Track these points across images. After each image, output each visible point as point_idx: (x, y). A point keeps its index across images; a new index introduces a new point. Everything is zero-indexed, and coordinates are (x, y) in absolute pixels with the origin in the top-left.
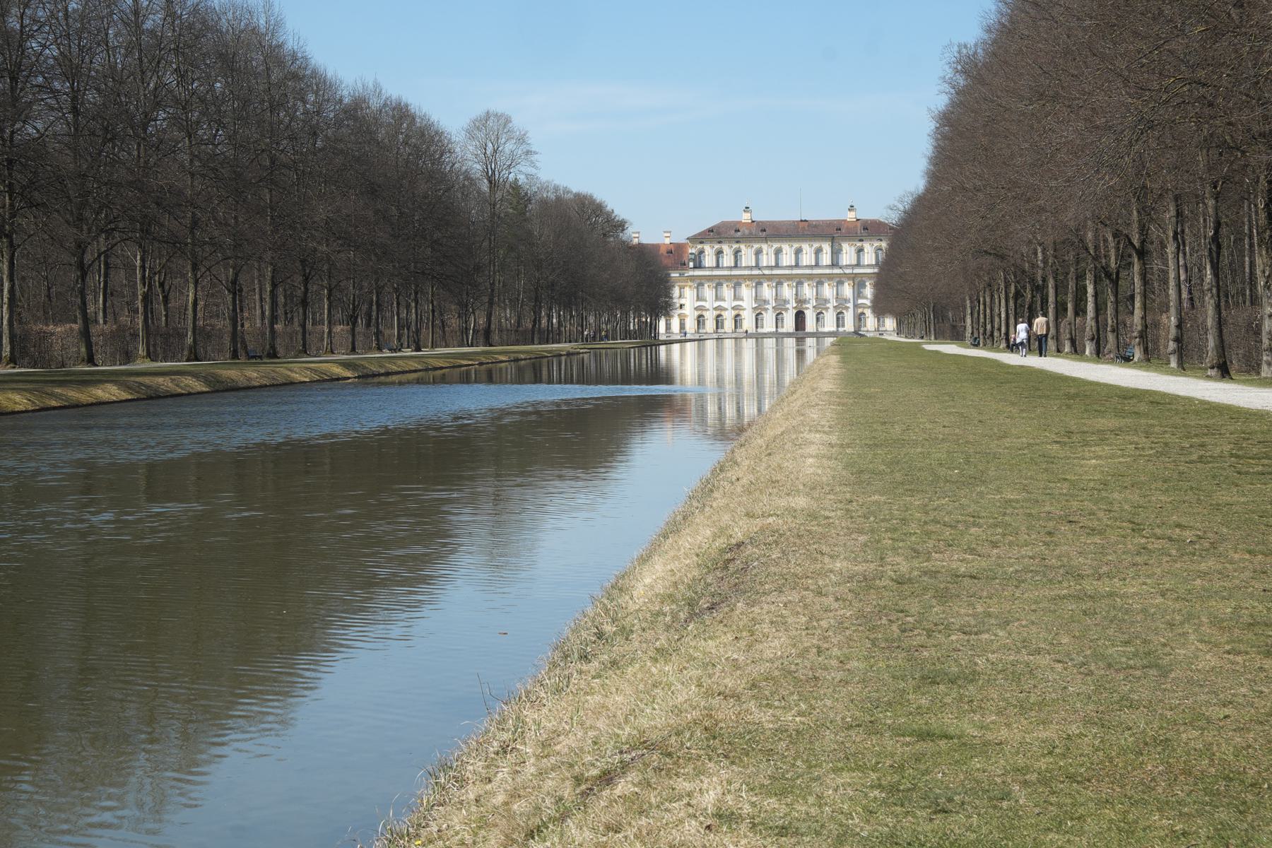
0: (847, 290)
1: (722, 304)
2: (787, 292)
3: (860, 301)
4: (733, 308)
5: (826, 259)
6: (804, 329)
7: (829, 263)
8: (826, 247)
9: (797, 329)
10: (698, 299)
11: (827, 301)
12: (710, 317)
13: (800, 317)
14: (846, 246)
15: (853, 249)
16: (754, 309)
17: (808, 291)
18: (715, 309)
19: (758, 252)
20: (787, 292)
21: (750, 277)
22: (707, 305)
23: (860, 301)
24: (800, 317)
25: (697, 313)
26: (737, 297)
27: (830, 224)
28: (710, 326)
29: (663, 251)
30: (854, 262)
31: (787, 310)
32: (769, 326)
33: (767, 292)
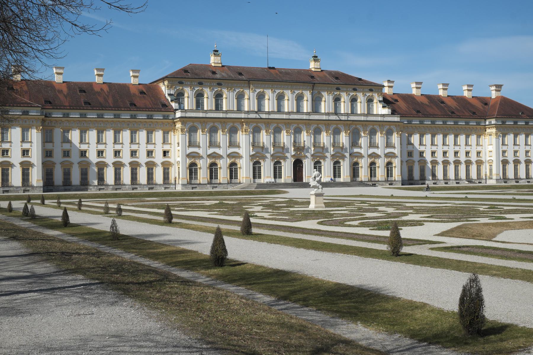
0: (344, 139)
1: (217, 150)
2: (285, 138)
3: (356, 150)
4: (229, 156)
5: (306, 106)
6: (301, 179)
7: (310, 110)
8: (307, 95)
9: (295, 179)
10: (191, 144)
11: (324, 149)
12: (203, 165)
13: (298, 165)
14: (325, 94)
15: (331, 97)
16: (252, 157)
17: (305, 138)
18: (209, 156)
19: (240, 97)
20: (285, 138)
21: (248, 121)
22: (200, 151)
23: (356, 150)
24: (298, 165)
25: (188, 161)
26: (232, 144)
27: (300, 72)
28: (203, 175)
29: (133, 91)
30: (332, 110)
31: (285, 158)
32: (267, 177)
33: (265, 138)
